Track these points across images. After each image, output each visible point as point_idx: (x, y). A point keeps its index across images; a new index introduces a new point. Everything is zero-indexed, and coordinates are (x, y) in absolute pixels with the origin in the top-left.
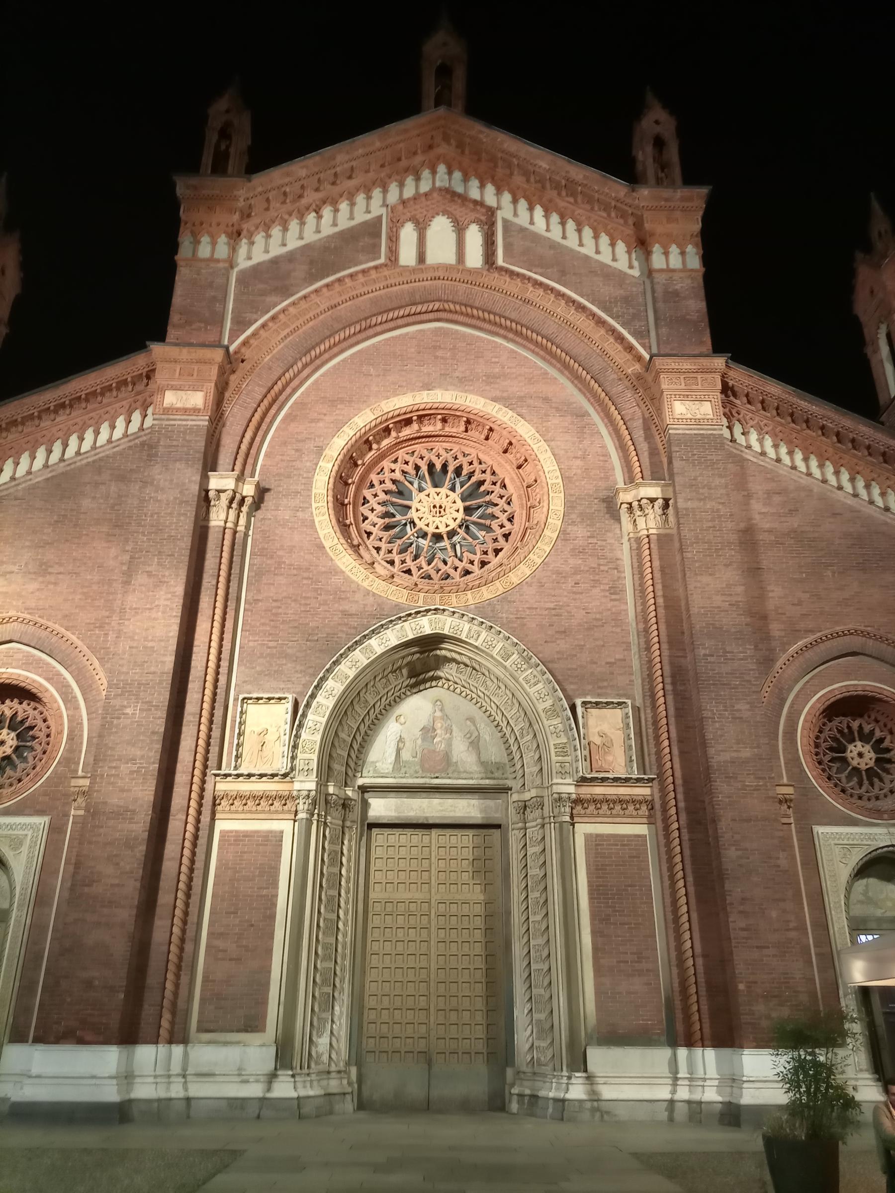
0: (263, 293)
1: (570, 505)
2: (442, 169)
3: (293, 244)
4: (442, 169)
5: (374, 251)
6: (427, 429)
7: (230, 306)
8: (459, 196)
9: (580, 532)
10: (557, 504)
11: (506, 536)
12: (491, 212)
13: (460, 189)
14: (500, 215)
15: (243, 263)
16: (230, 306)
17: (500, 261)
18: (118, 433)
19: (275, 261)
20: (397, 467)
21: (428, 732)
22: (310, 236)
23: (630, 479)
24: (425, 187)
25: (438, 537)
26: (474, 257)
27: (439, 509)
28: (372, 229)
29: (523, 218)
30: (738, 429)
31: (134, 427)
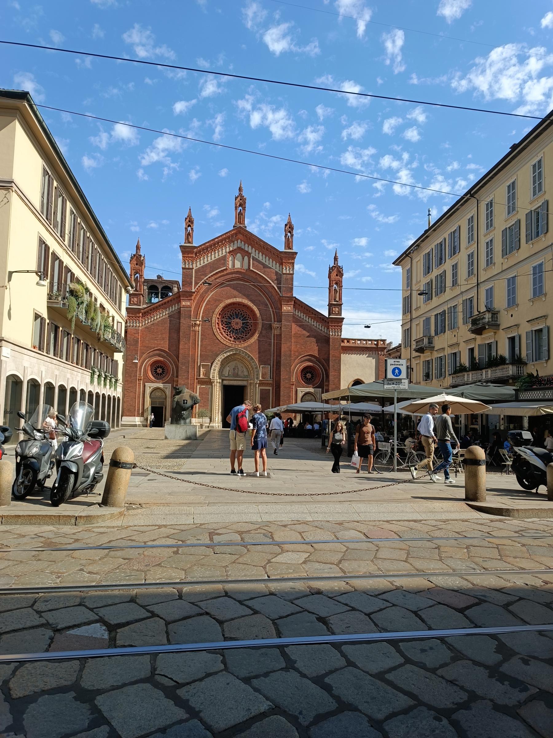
0: (201, 275)
1: (263, 326)
2: (239, 241)
3: (206, 263)
4: (239, 241)
5: (224, 264)
6: (235, 306)
7: (194, 278)
8: (242, 249)
9: (264, 332)
10: (260, 326)
11: (250, 330)
12: (250, 254)
13: (243, 247)
14: (252, 255)
15: (195, 268)
16: (194, 278)
17: (251, 268)
18: (173, 309)
19: (203, 267)
20: (229, 313)
21: (234, 369)
22: (210, 261)
23: (275, 321)
24: (235, 247)
25: (237, 330)
26: (246, 267)
27: (237, 323)
28: (224, 258)
29: (257, 257)
30: (297, 311)
31: (176, 308)
